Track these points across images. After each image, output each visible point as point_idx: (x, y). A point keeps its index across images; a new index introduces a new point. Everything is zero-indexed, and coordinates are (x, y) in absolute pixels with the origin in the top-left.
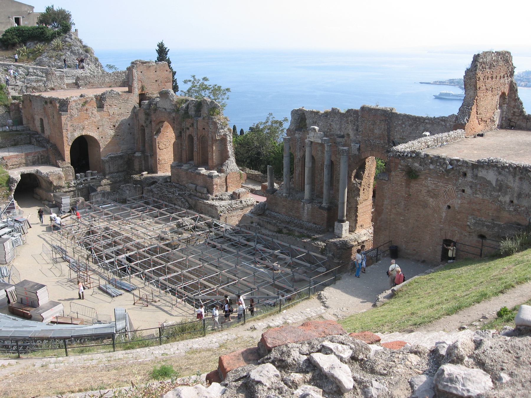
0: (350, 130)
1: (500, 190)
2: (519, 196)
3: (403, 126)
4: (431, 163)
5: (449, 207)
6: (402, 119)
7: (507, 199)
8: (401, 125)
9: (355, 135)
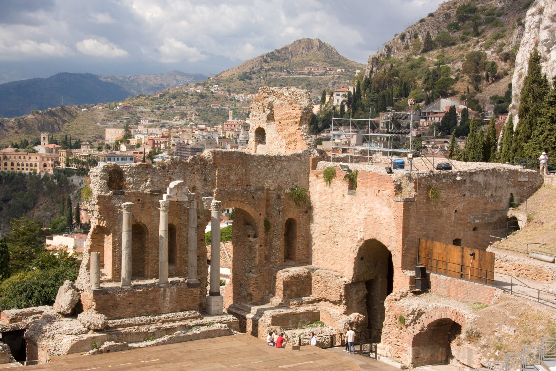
0: (197, 182)
1: (485, 189)
2: (496, 190)
3: (259, 167)
4: (444, 177)
5: (456, 211)
6: (257, 160)
7: (490, 194)
9: (204, 186)
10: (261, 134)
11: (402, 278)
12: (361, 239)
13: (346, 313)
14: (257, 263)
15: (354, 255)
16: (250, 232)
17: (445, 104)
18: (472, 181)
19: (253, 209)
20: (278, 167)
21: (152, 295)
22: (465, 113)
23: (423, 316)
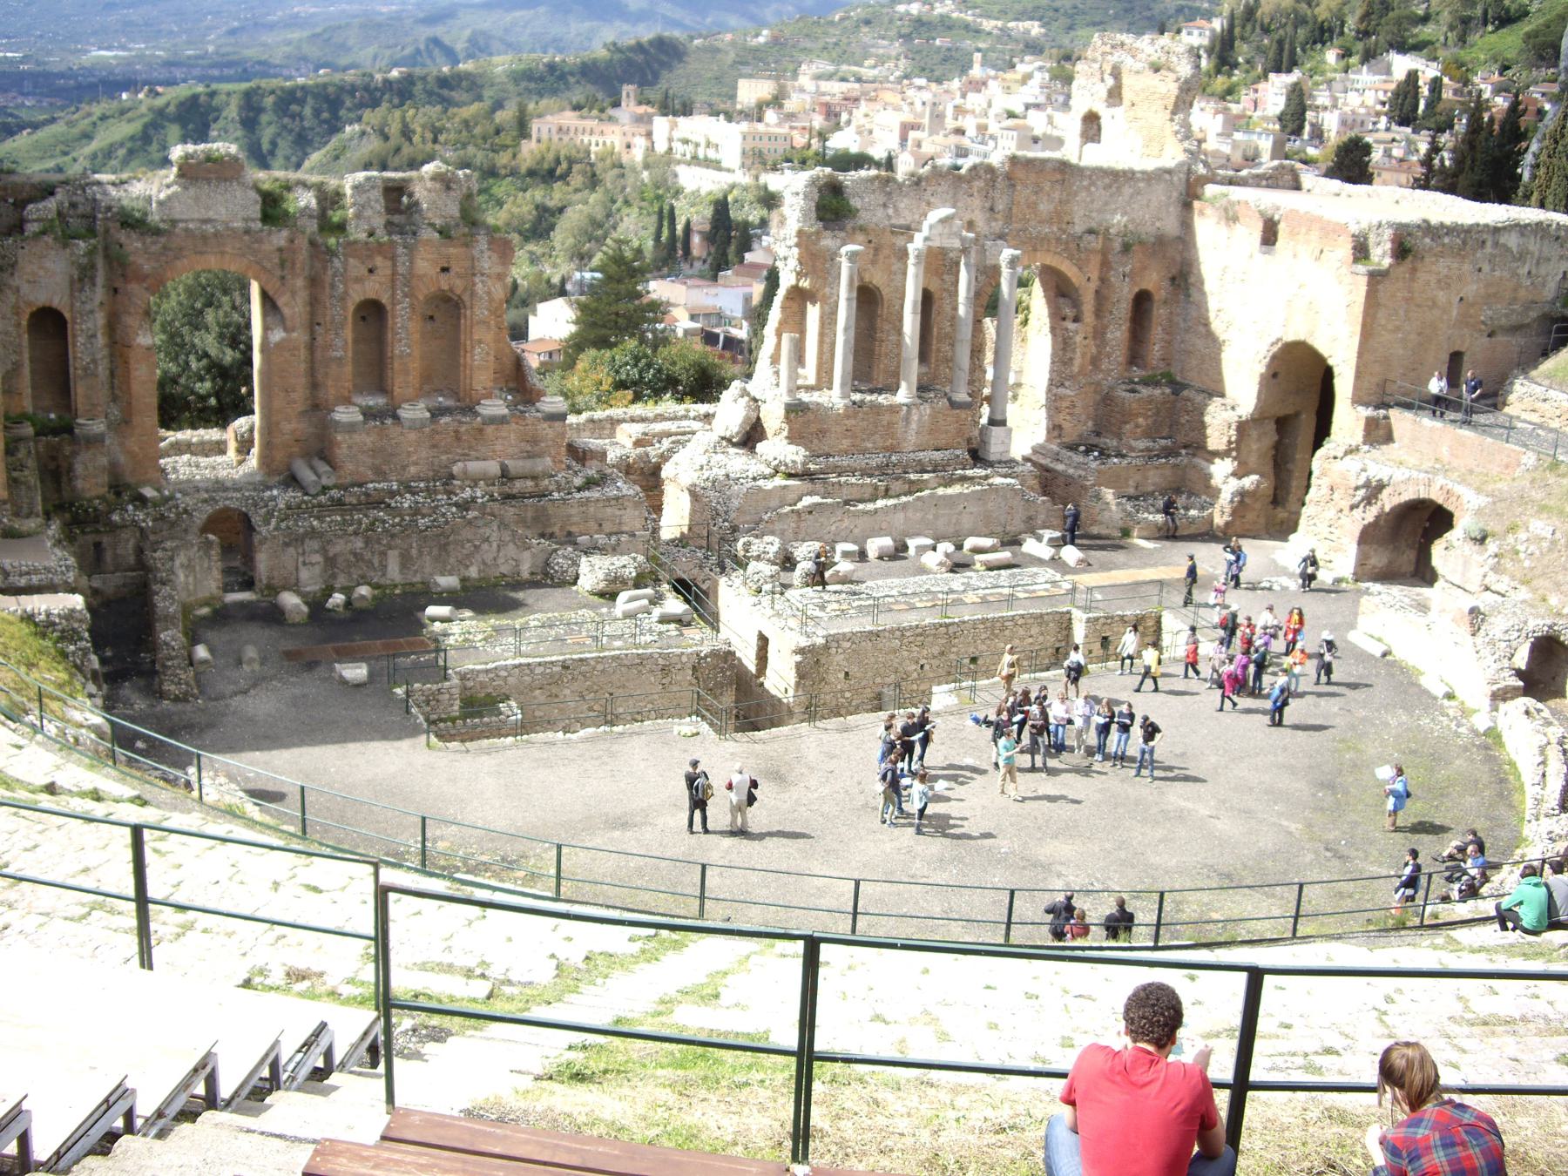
0: (977, 212)
2: (1538, 263)
7: (1526, 270)
8: (1087, 189)
9: (989, 221)
10: (1092, 125)
11: (1348, 419)
12: (1279, 340)
13: (1234, 474)
14: (1076, 369)
15: (1261, 369)
16: (1069, 312)
17: (1401, 64)
18: (1496, 244)
19: (1075, 269)
20: (1127, 191)
21: (886, 418)
22: (1436, 85)
23: (1385, 492)
